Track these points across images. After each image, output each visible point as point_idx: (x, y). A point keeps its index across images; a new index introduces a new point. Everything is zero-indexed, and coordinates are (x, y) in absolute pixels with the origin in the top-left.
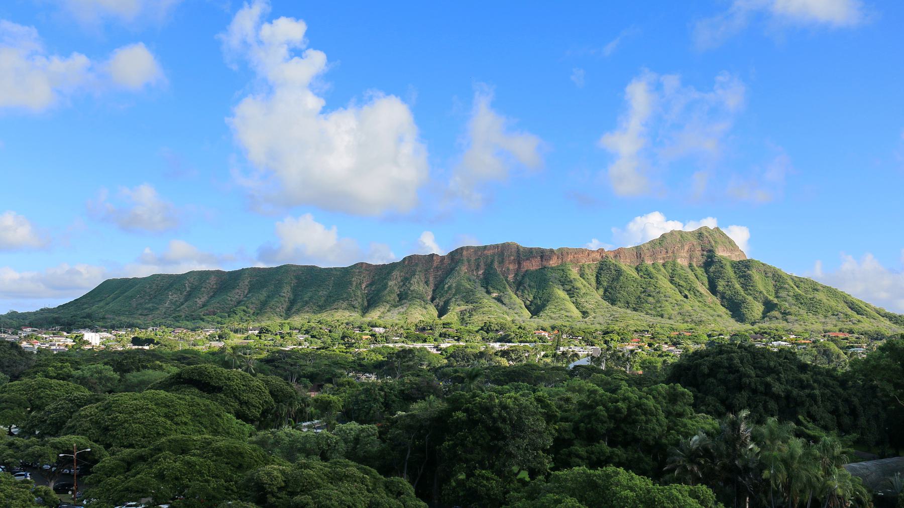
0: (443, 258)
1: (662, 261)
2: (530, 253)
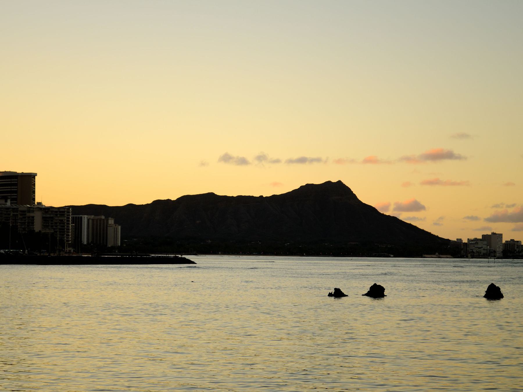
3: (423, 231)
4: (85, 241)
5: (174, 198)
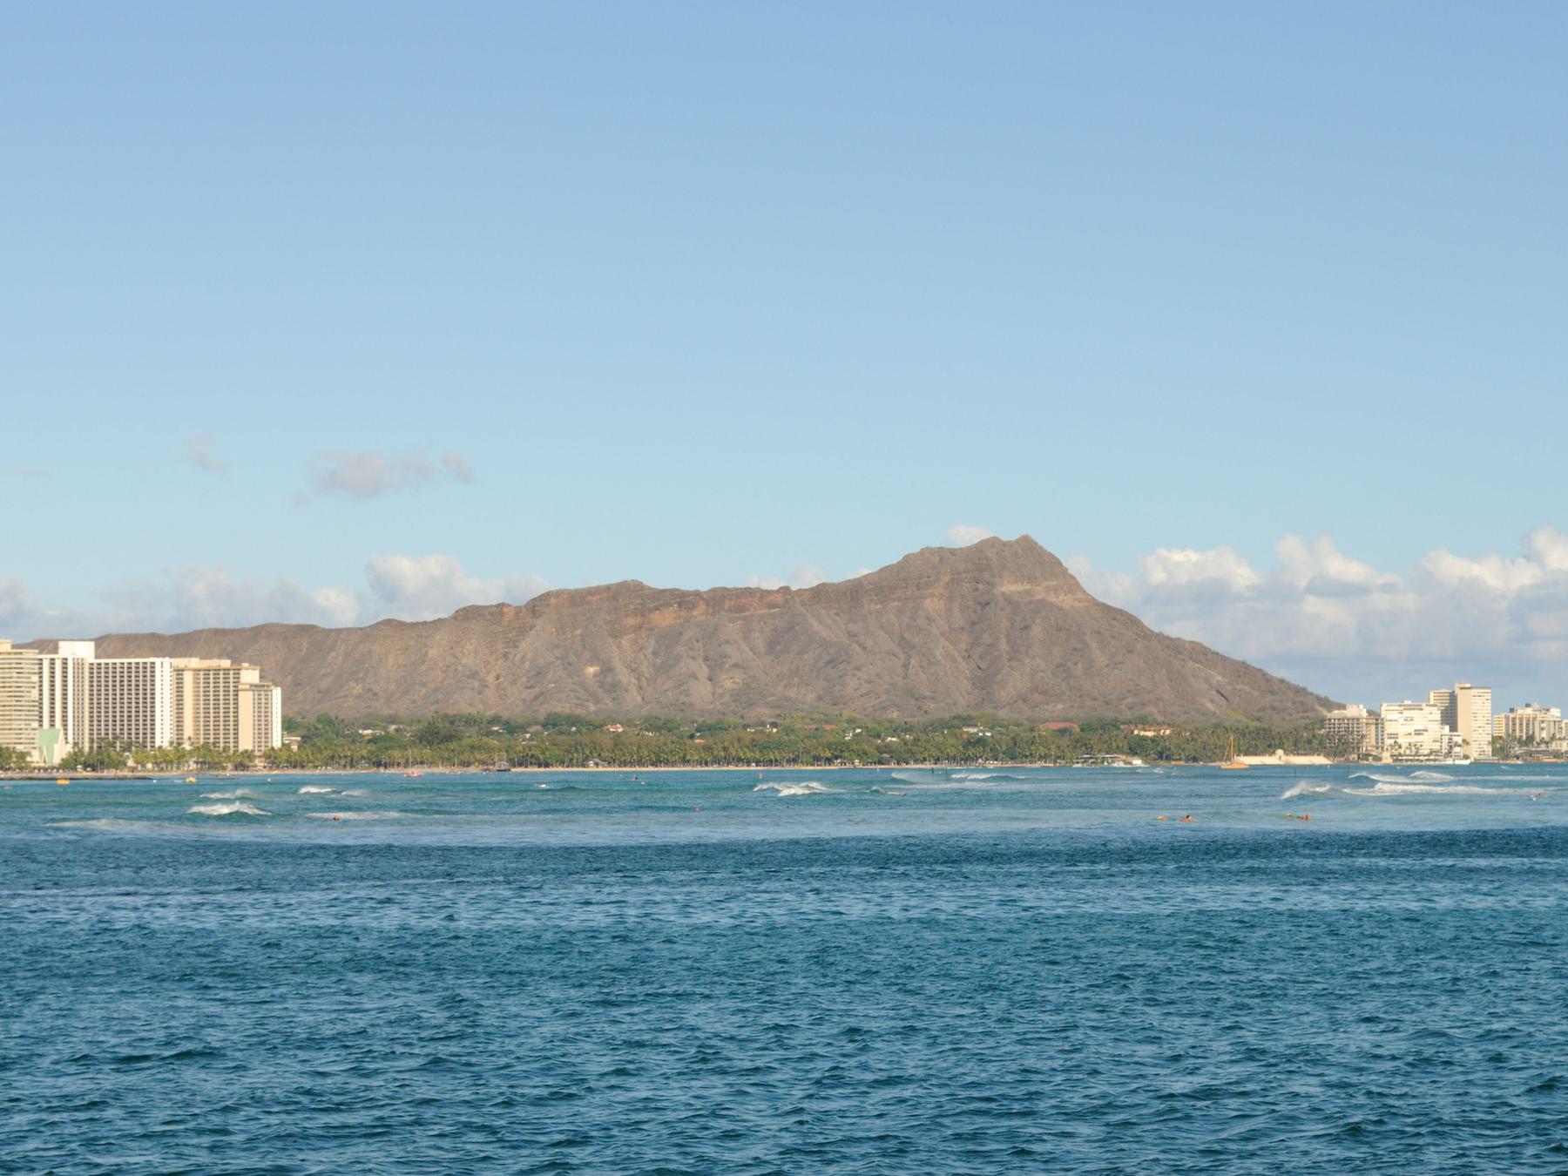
0: (518, 610)
3: (1282, 681)
4: (164, 736)
5: (522, 600)
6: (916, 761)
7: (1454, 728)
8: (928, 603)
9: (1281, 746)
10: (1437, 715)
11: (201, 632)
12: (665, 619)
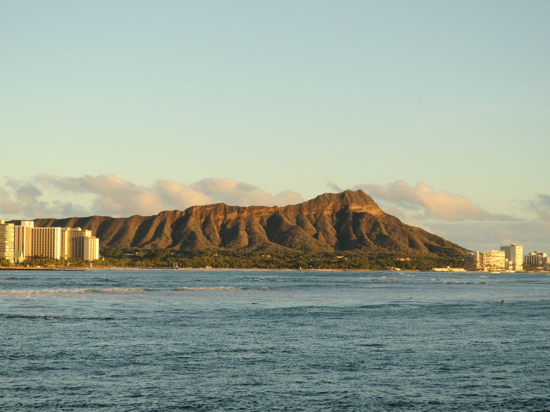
0: (182, 212)
1: (306, 213)
2: (232, 209)
4: (58, 256)
6: (321, 268)
7: (509, 260)
8: (325, 212)
9: (448, 265)
10: (504, 255)
11: (70, 218)
12: (233, 216)
